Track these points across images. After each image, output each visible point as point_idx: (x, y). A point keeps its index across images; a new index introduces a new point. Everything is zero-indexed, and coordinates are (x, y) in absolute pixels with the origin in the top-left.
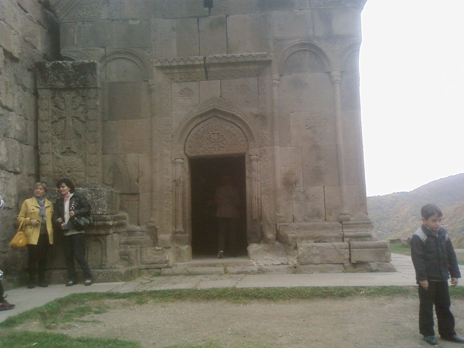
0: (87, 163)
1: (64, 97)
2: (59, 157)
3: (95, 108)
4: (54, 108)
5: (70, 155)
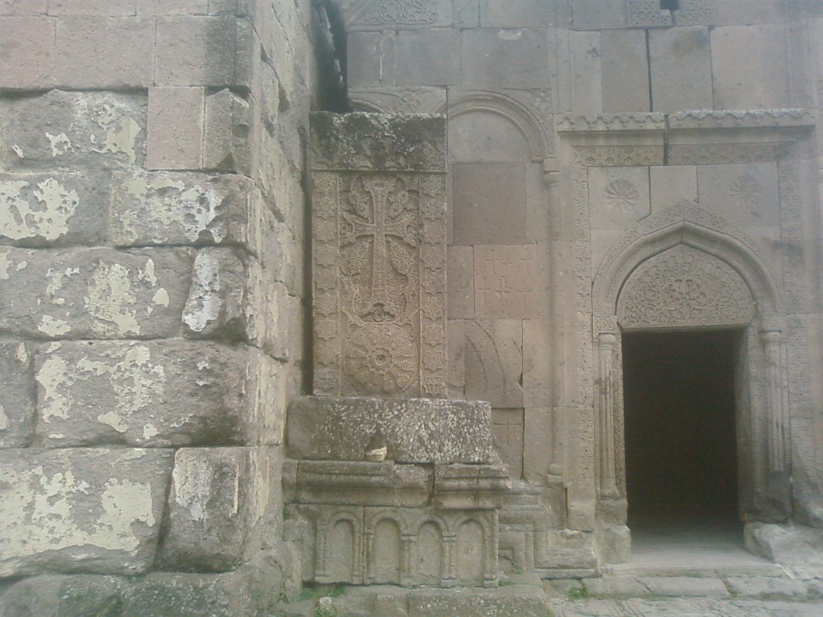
0: (422, 340)
1: (369, 192)
2: (358, 324)
4: (345, 215)
5: (381, 321)
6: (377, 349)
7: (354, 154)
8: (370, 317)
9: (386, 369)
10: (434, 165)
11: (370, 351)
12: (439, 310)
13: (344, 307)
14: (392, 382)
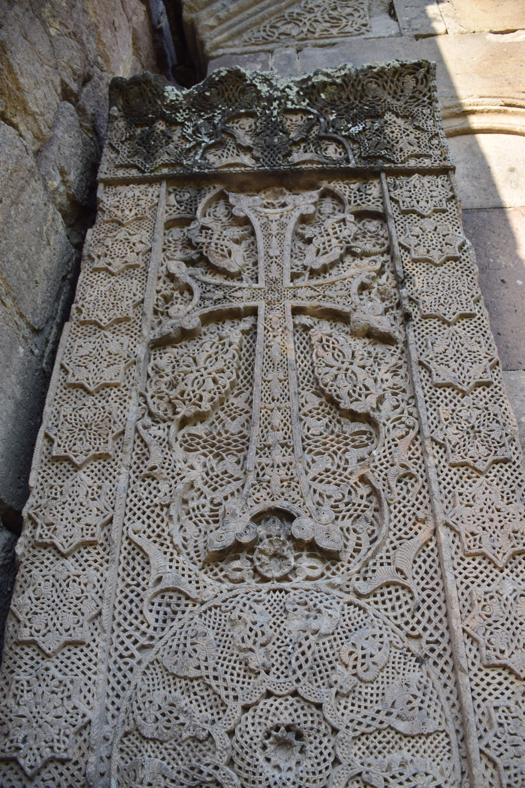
1: (246, 221)
2: (191, 590)
3: (456, 259)
5: (285, 578)
6: (269, 694)
7: (208, 147)
8: (237, 564)
10: (418, 156)
13: (138, 525)
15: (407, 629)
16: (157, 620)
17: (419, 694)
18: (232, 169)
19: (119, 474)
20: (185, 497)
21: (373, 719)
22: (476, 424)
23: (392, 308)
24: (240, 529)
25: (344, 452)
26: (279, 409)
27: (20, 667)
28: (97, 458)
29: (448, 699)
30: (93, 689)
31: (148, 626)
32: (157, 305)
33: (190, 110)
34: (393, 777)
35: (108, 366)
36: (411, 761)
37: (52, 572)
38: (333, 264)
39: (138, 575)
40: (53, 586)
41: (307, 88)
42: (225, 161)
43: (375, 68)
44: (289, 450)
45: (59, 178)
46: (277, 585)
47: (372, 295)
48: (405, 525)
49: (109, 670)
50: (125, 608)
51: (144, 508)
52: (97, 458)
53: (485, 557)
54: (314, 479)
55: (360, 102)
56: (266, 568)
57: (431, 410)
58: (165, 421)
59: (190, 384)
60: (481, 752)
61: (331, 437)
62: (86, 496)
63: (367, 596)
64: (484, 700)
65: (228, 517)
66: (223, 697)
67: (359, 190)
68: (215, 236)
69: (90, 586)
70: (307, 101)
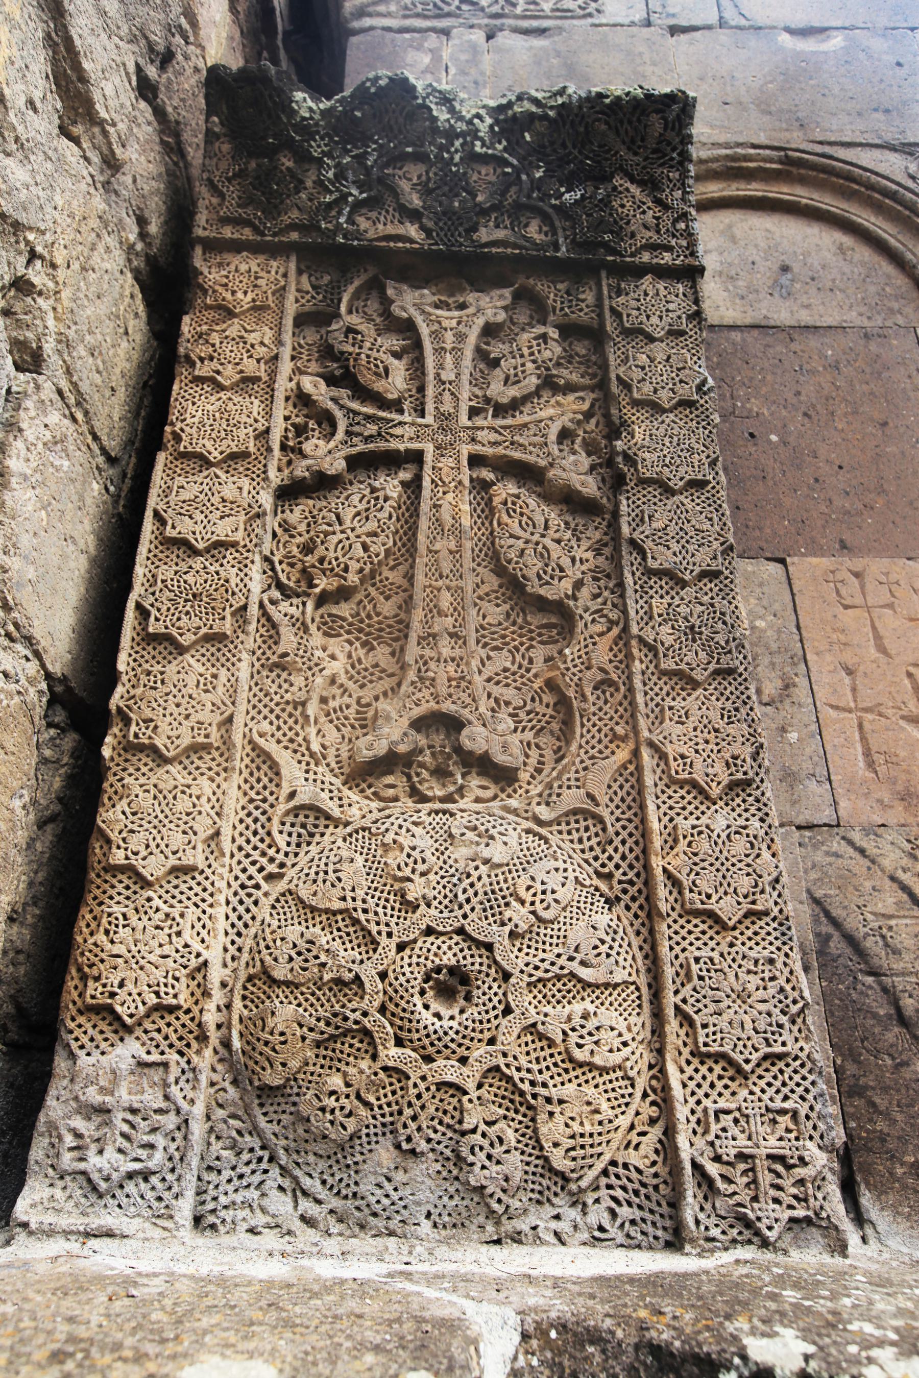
0: (662, 892)
5: (449, 799)
6: (429, 931)
8: (389, 780)
9: (479, 1051)
10: (653, 247)
11: (388, 945)
12: (736, 749)
13: (265, 726)
14: (511, 1136)
15: (597, 864)
16: (289, 844)
17: (608, 939)
18: (392, 244)
19: (240, 660)
20: (324, 694)
21: (553, 964)
22: (698, 623)
23: (601, 465)
24: (395, 737)
25: (528, 649)
26: (448, 588)
27: (111, 898)
28: (209, 638)
29: (641, 948)
30: (209, 925)
31: (278, 851)
32: (286, 438)
33: (331, 139)
34: (573, 1030)
35: (222, 517)
36: (595, 1014)
37: (153, 780)
38: (526, 399)
39: (265, 788)
40: (155, 798)
41: (505, 121)
42: (381, 229)
43: (607, 97)
44: (460, 642)
45: (136, 230)
46: (438, 806)
47: (576, 447)
48: (600, 742)
49: (228, 903)
50: (247, 828)
51: (272, 704)
52: (209, 638)
53: (694, 784)
54: (489, 680)
55: (580, 152)
56: (426, 785)
57: (641, 602)
58: (298, 596)
59: (332, 548)
60: (677, 1007)
61: (512, 629)
62: (197, 686)
63: (548, 824)
64: (684, 950)
65: (380, 722)
66: (374, 932)
67: (568, 293)
68: (368, 345)
69: (204, 800)
70: (504, 143)
